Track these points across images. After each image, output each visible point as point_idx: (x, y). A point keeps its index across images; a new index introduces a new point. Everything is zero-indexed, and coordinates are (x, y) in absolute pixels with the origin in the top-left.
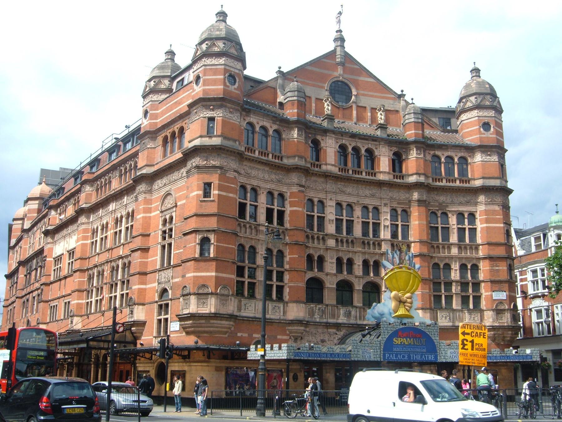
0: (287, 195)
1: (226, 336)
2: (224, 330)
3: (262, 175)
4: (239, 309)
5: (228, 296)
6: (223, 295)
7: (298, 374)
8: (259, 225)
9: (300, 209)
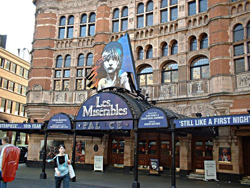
0: (96, 12)
1: (43, 118)
2: (38, 114)
3: (76, 5)
4: (53, 100)
5: (40, 91)
6: (36, 91)
7: (99, 146)
8: (73, 39)
9: (102, 18)
